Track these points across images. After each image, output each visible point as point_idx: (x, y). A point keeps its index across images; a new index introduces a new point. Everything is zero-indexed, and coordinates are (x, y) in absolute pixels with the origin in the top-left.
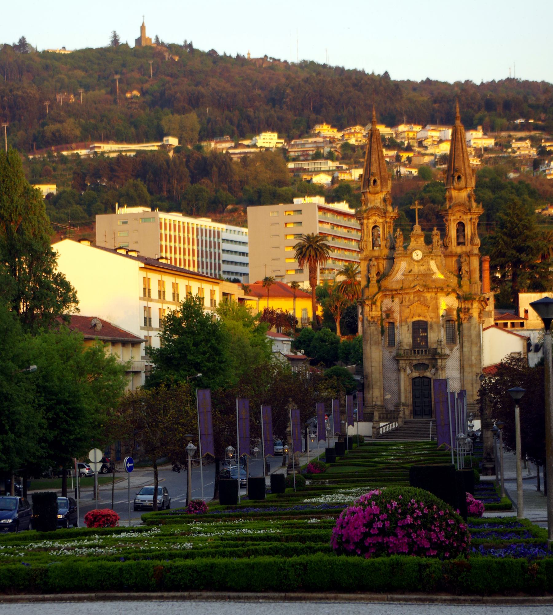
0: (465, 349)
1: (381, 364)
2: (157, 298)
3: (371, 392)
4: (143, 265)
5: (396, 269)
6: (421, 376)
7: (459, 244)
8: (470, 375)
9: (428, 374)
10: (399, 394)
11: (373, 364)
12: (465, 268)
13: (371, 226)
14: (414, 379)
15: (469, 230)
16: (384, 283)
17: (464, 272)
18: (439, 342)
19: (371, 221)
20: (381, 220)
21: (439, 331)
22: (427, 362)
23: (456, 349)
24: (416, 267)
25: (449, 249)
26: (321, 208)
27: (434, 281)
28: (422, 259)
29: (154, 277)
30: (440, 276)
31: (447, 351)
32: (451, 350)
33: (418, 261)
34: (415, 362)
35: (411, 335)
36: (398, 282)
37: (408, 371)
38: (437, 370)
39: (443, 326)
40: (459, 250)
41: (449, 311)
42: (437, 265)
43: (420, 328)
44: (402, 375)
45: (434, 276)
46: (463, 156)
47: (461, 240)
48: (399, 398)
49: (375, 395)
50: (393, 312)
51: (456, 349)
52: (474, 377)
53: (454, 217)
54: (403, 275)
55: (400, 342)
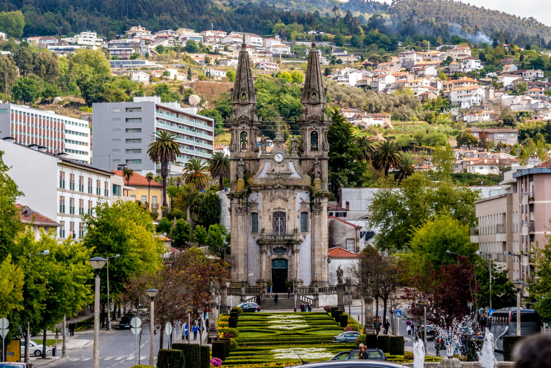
0: (316, 236)
1: (246, 247)
2: (69, 189)
3: (237, 270)
4: (61, 161)
5: (261, 168)
6: (280, 258)
7: (313, 149)
8: (320, 257)
9: (285, 256)
10: (261, 273)
11: (239, 247)
12: (317, 169)
13: (239, 132)
14: (273, 260)
15: (321, 138)
16: (251, 180)
17: (316, 172)
18: (295, 230)
19: (240, 128)
20: (248, 128)
21: (295, 221)
22: (284, 247)
23: (308, 236)
24: (277, 167)
25: (305, 154)
26: (158, 107)
28: (283, 161)
29: (68, 171)
30: (296, 175)
31: (301, 237)
32: (305, 237)
33: (279, 163)
34: (274, 247)
35: (272, 223)
36: (261, 179)
37: (269, 253)
38: (293, 253)
39: (298, 217)
40: (312, 154)
41: (303, 203)
42: (295, 167)
44: (264, 256)
45: (292, 176)
46: (318, 77)
47: (315, 146)
48: (261, 276)
49: (239, 273)
50: (258, 204)
51: (308, 236)
52: (323, 260)
53: (309, 127)
54: (267, 174)
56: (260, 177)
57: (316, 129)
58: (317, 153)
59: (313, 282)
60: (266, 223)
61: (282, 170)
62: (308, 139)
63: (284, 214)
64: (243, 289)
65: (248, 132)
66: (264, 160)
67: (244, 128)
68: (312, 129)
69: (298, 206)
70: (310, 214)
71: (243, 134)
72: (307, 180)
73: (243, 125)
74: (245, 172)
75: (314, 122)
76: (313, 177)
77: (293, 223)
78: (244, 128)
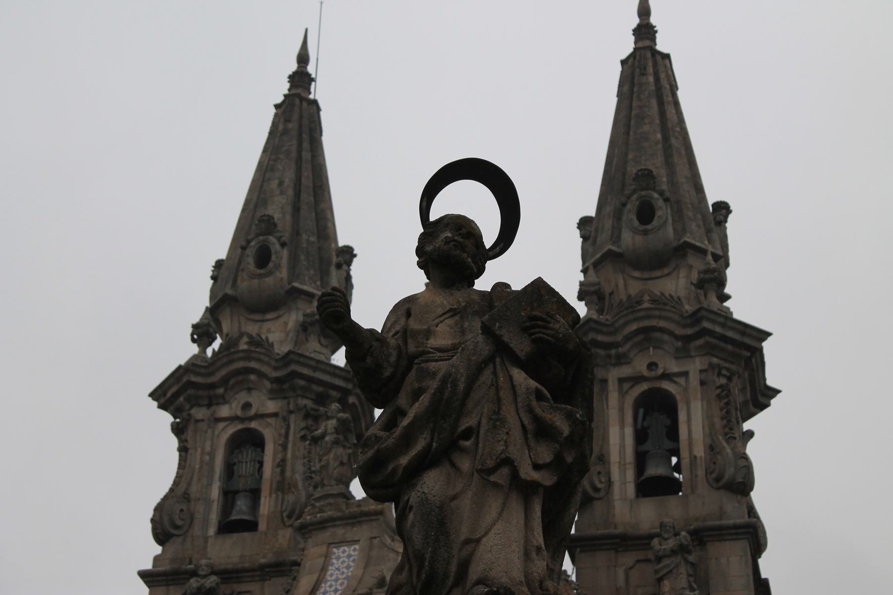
19: (224, 411)
20: (271, 406)
40: (647, 515)
53: (625, 371)
57: (666, 376)
58: (673, 509)
62: (614, 433)
65: (269, 435)
66: (325, 536)
67: (247, 406)
68: (637, 379)
71: (247, 441)
73: (243, 397)
75: (647, 337)
78: (247, 406)
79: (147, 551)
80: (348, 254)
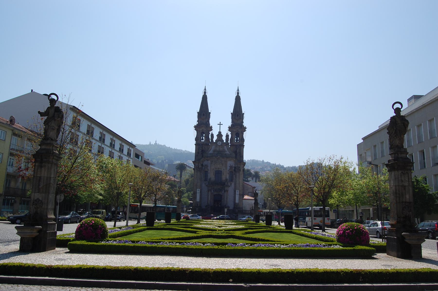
9: (221, 193)
18: (226, 180)
27: (226, 154)
30: (228, 152)
33: (219, 146)
38: (225, 191)
41: (231, 167)
43: (218, 173)
44: (210, 193)
55: (210, 179)
56: (209, 153)
59: (234, 208)
60: (211, 176)
61: (221, 149)
63: (221, 171)
64: (197, 209)
69: (228, 168)
70: (234, 172)
72: (234, 155)
74: (202, 151)
76: (236, 155)
77: (225, 176)
79: (195, 142)
80: (210, 113)
